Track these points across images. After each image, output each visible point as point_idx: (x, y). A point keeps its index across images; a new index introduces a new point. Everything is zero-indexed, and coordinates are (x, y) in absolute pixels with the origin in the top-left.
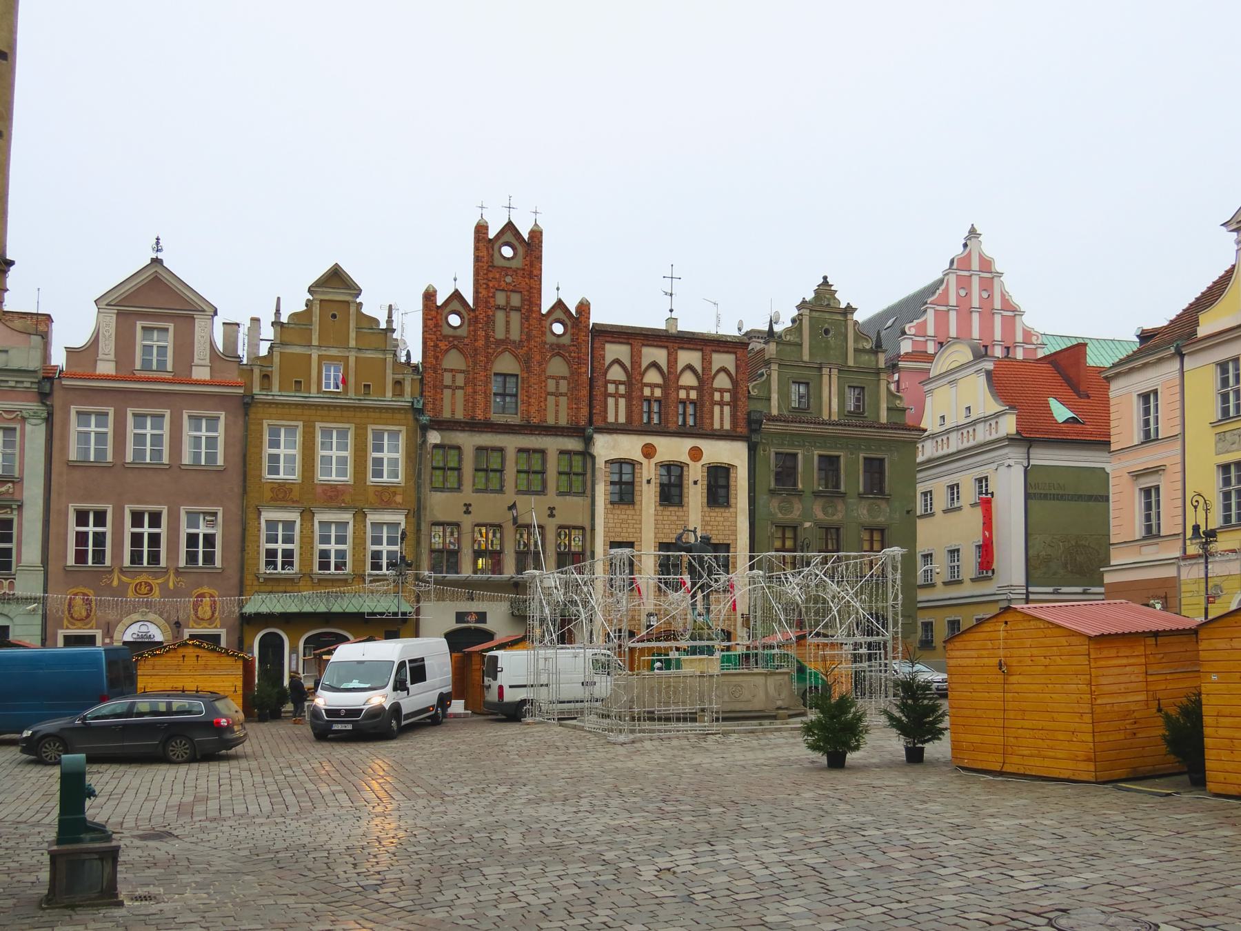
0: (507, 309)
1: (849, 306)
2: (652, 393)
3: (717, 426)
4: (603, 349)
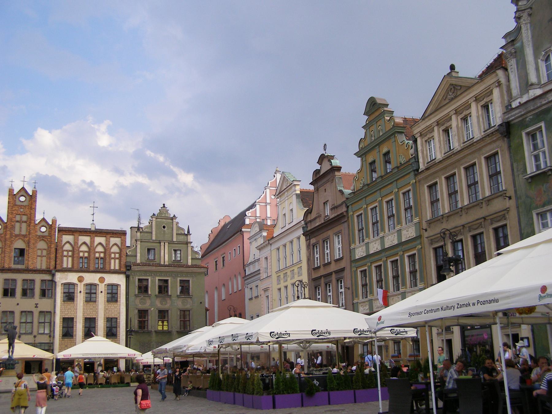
1: (174, 216)
2: (100, 255)
3: (112, 268)
4: (62, 237)
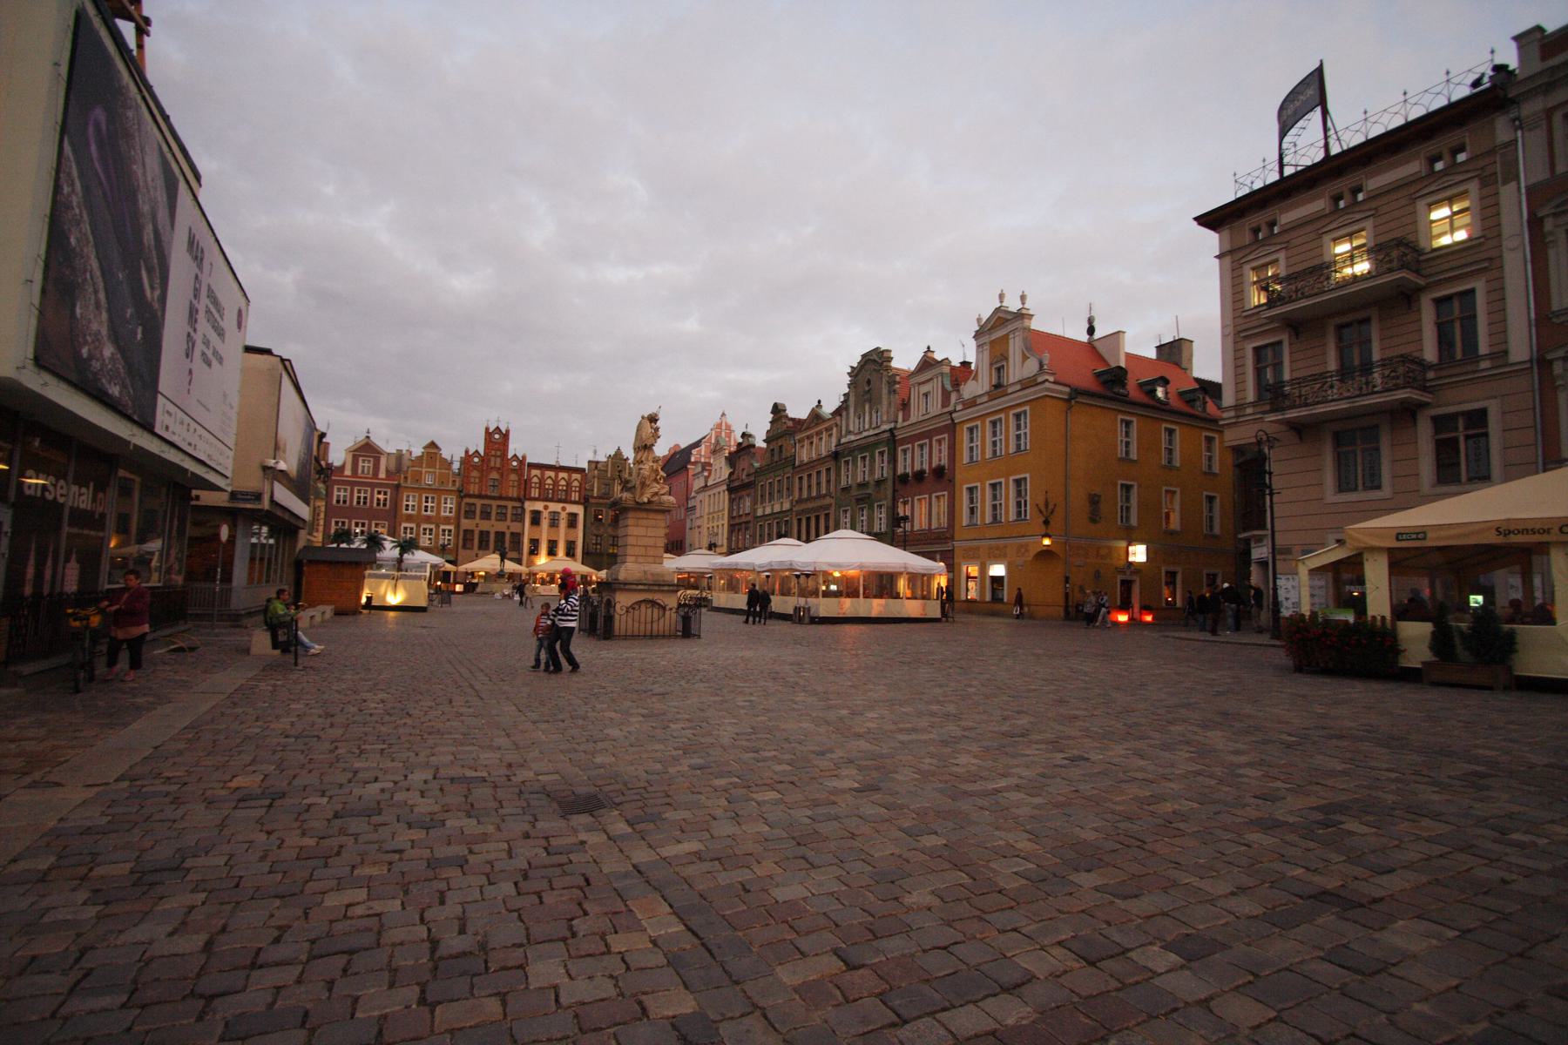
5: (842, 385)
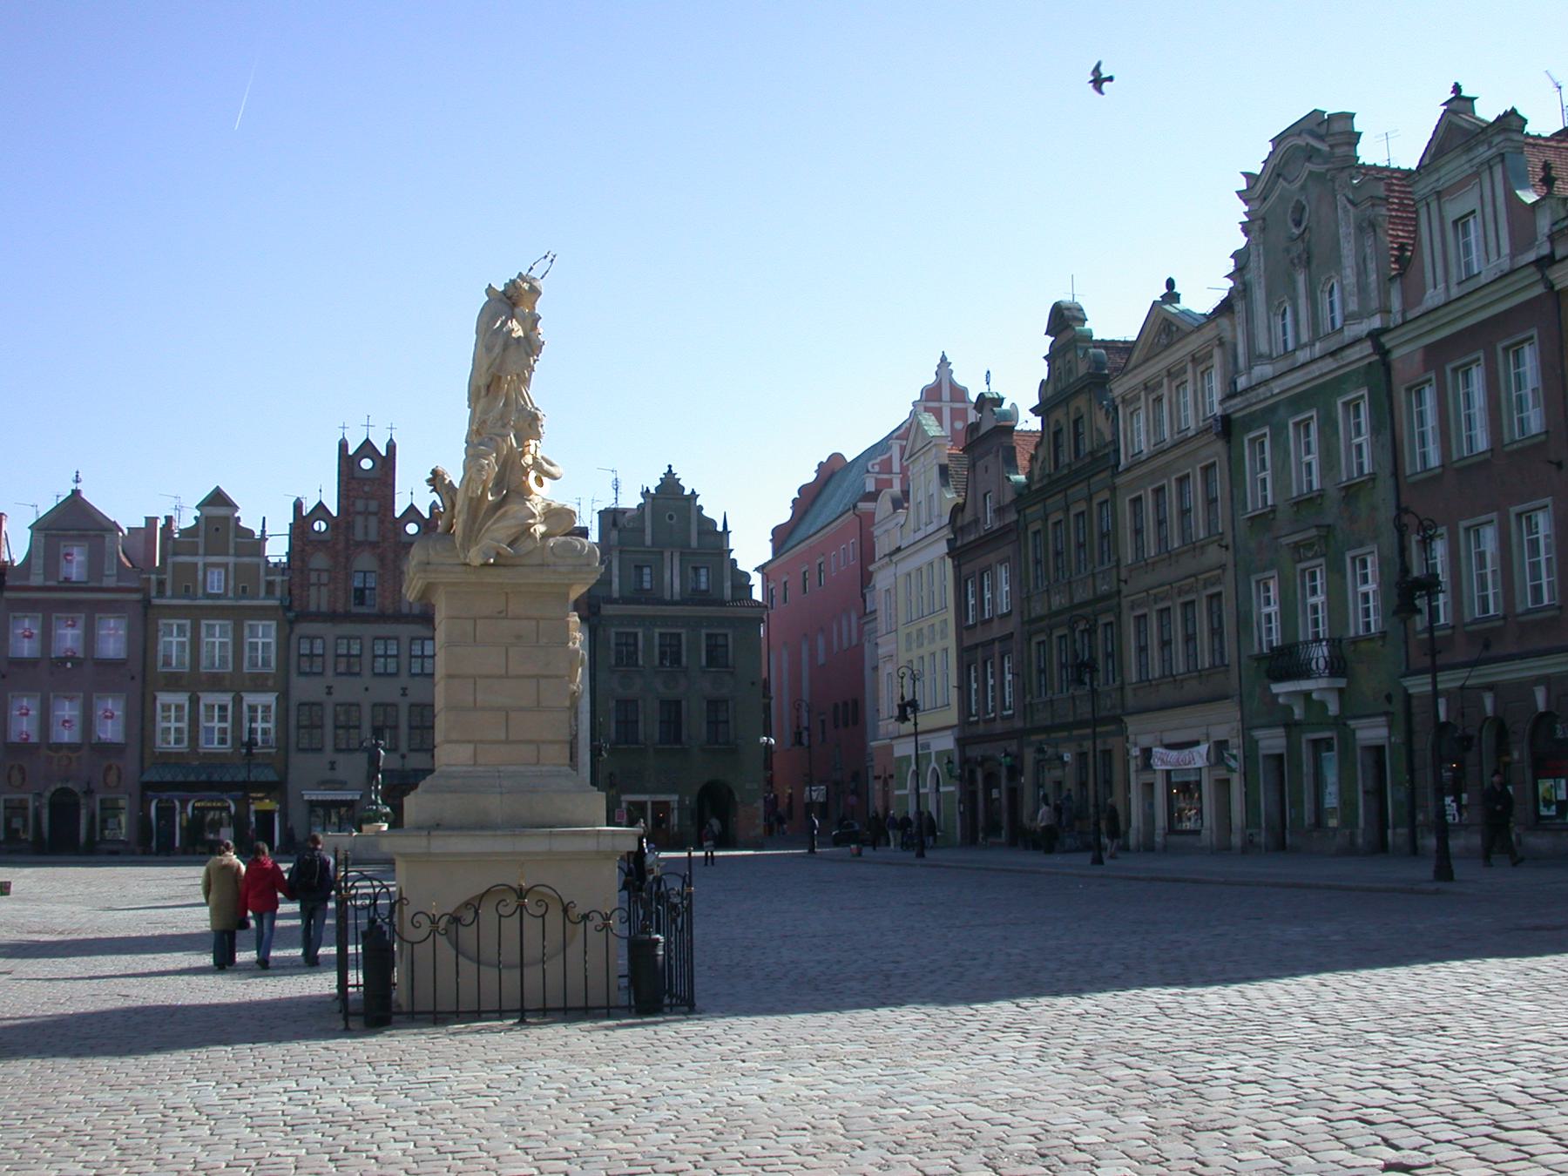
0: (366, 513)
5: (1225, 229)
